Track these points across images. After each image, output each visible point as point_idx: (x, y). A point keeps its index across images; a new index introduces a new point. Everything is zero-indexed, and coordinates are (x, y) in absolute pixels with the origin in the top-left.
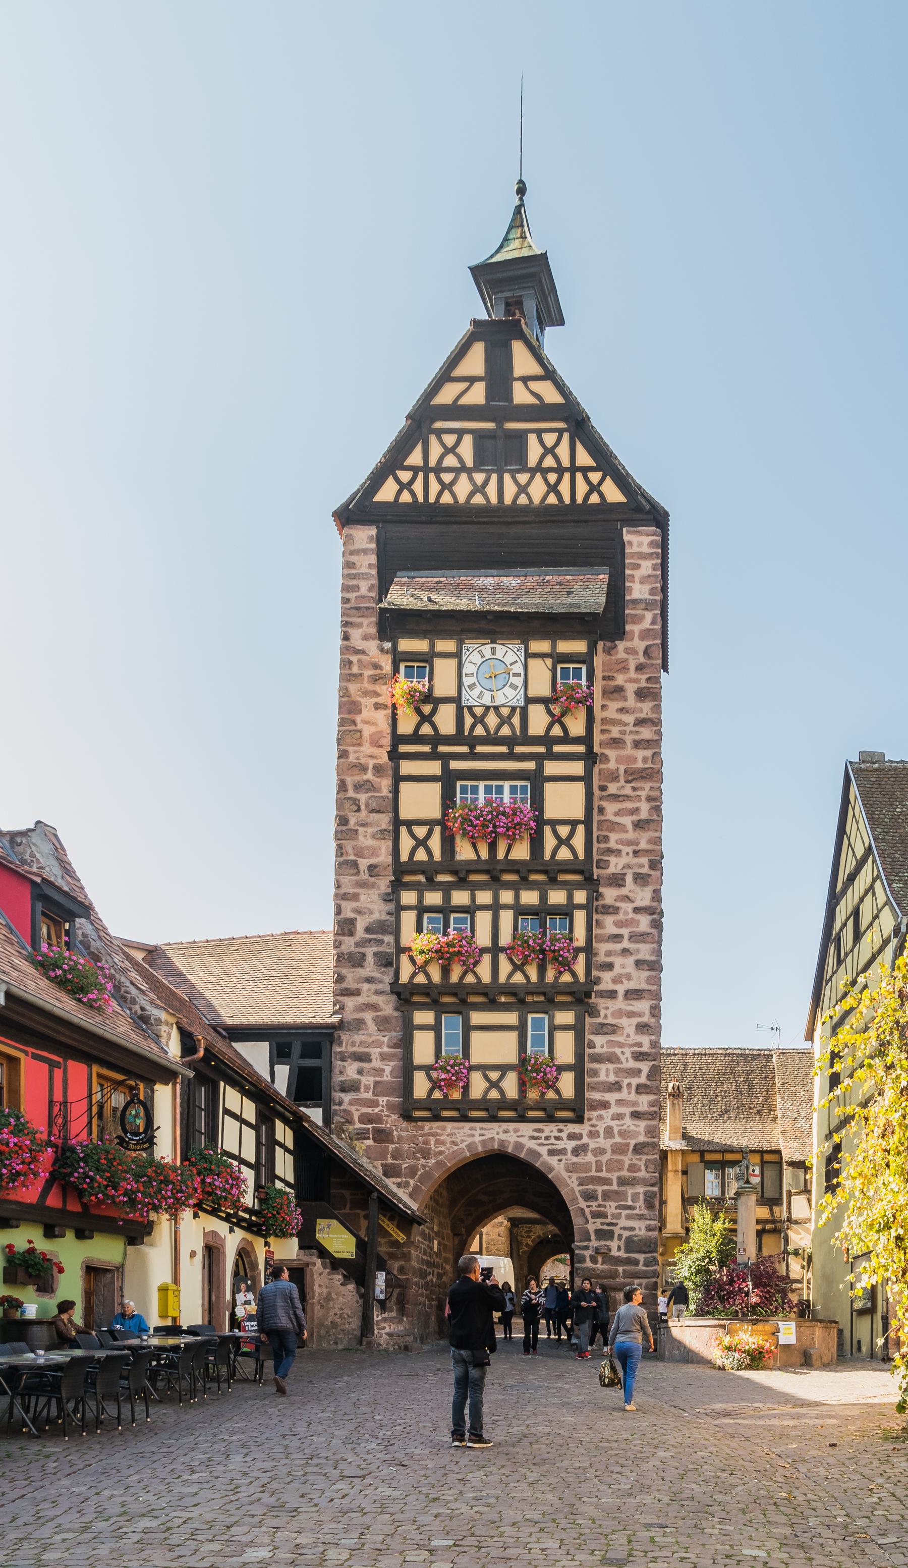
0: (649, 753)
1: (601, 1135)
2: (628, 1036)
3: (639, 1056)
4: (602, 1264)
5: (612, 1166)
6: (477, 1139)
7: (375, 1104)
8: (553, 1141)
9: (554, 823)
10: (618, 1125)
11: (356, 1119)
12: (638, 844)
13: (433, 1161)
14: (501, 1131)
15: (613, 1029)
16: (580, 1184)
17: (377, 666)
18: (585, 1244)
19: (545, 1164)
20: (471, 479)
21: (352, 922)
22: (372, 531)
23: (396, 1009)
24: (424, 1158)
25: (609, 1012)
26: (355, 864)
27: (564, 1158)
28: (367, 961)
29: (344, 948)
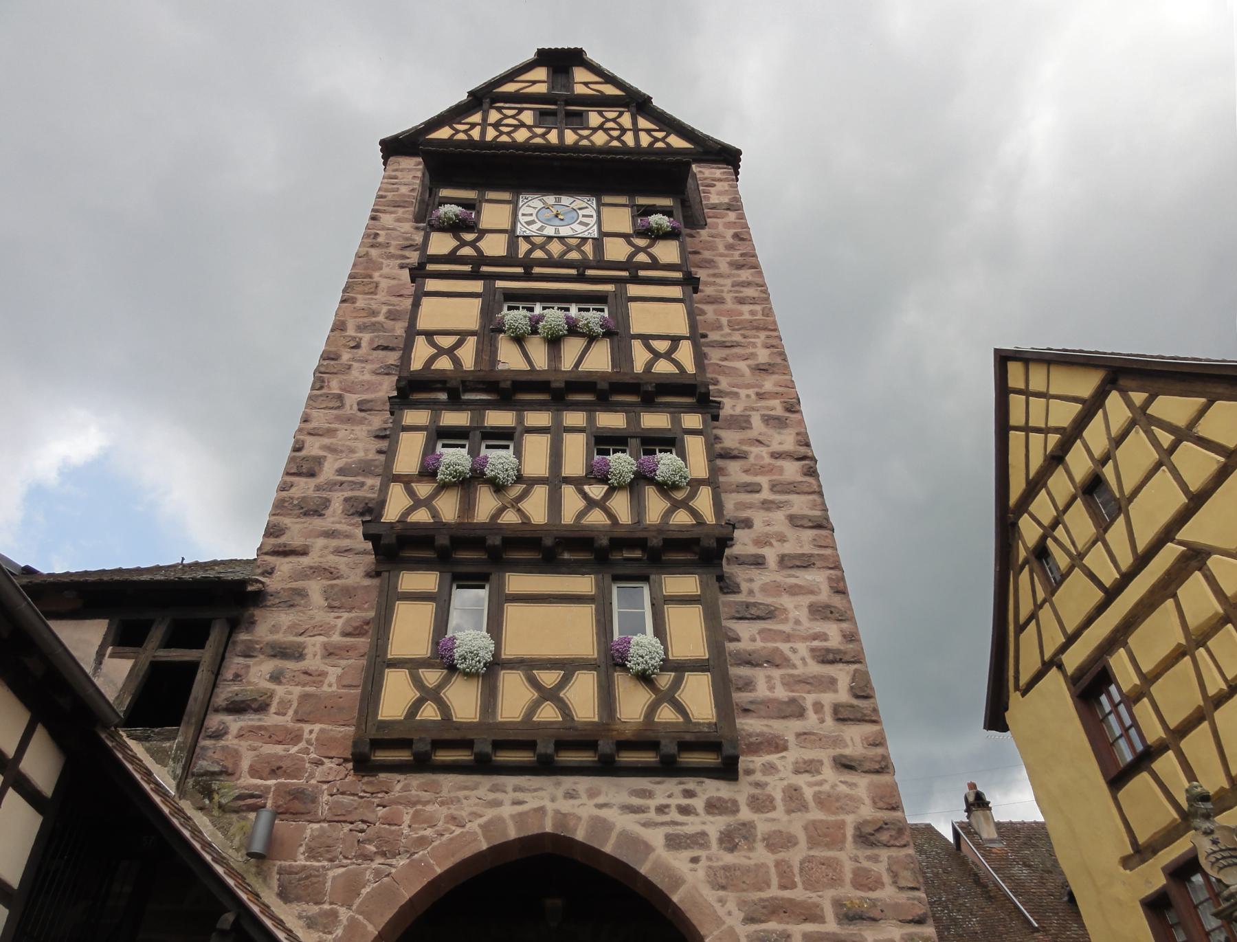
0: (758, 308)
2: (797, 622)
3: (828, 657)
5: (820, 873)
6: (507, 811)
7: (296, 738)
8: (674, 815)
9: (645, 339)
11: (245, 765)
12: (761, 386)
13: (402, 862)
14: (560, 793)
15: (769, 614)
16: (750, 920)
21: (319, 461)
23: (368, 575)
24: (384, 854)
26: (340, 397)
27: (702, 853)
28: (331, 509)
29: (296, 492)
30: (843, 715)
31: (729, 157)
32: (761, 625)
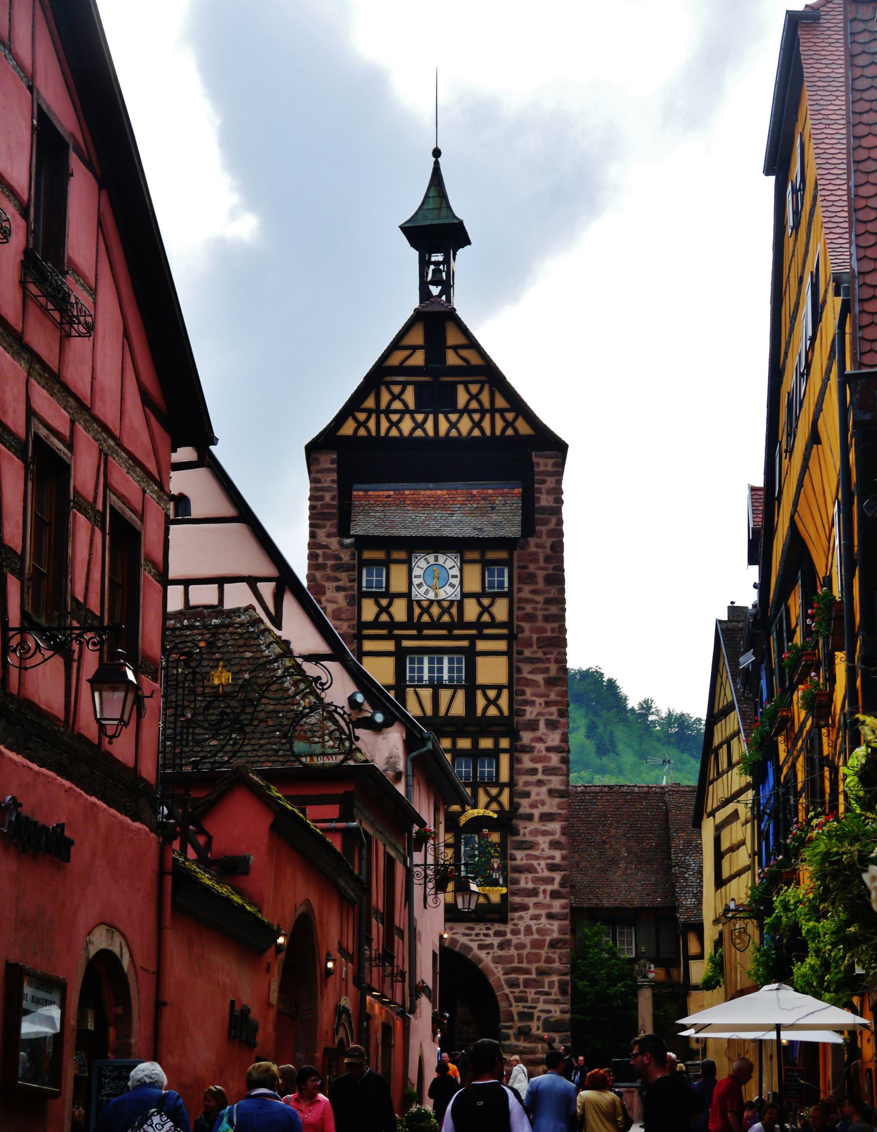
0: (556, 625)
2: (543, 850)
3: (552, 868)
4: (524, 1041)
8: (482, 937)
10: (536, 924)
12: (548, 696)
15: (532, 846)
16: (505, 974)
17: (338, 558)
18: (509, 1024)
19: (477, 956)
20: (414, 419)
22: (335, 456)
25: (527, 831)
27: (491, 951)
30: (555, 895)
31: (557, 448)
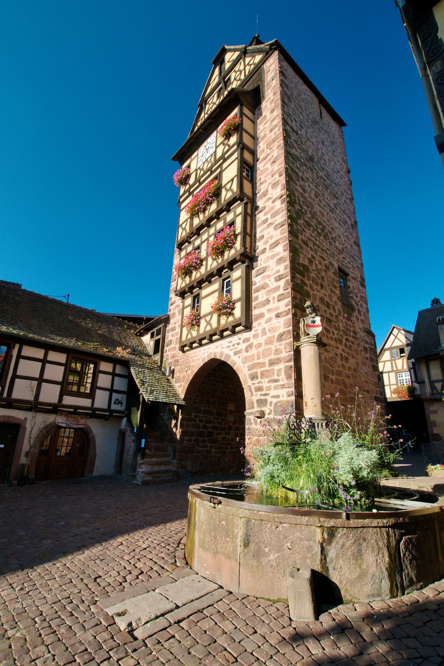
1: (260, 335)
8: (236, 346)
10: (268, 326)
16: (249, 370)
32: (262, 275)
